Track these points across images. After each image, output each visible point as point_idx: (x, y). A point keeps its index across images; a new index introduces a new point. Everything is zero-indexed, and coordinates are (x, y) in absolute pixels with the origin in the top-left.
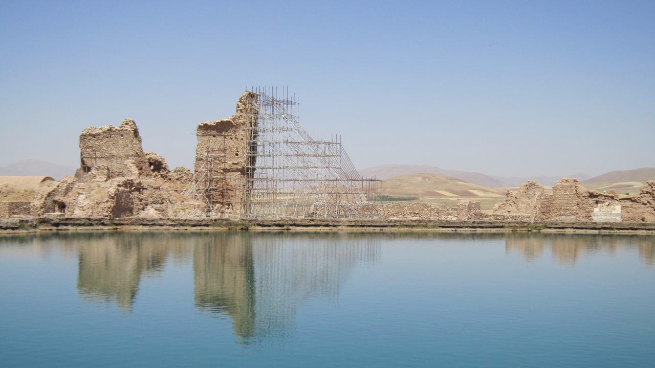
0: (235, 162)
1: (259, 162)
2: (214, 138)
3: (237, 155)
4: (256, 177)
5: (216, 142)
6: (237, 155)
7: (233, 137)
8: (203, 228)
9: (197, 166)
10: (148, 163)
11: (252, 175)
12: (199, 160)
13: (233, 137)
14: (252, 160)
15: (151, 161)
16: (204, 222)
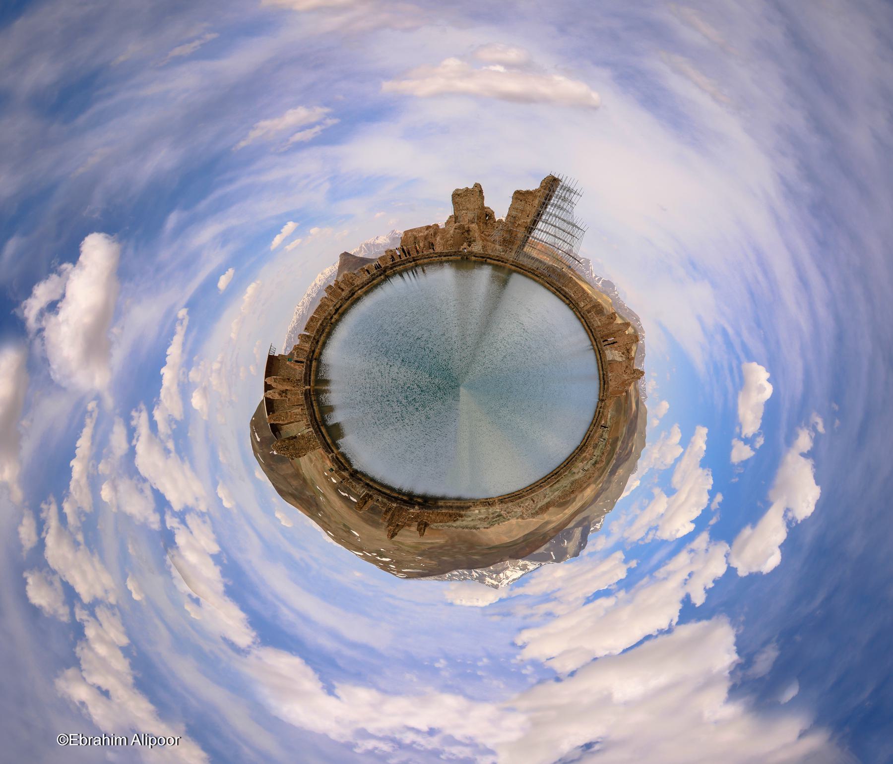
0: (525, 221)
1: (540, 225)
2: (521, 202)
3: (528, 216)
4: (535, 236)
5: (521, 204)
6: (528, 216)
7: (531, 204)
8: (449, 257)
9: (507, 218)
10: (485, 215)
11: (530, 233)
12: (508, 215)
13: (531, 204)
14: (535, 222)
15: (487, 213)
16: (449, 253)
